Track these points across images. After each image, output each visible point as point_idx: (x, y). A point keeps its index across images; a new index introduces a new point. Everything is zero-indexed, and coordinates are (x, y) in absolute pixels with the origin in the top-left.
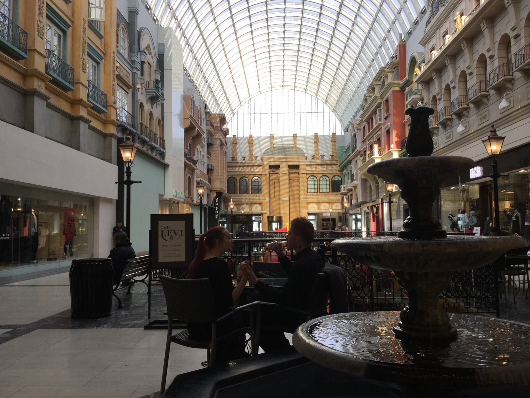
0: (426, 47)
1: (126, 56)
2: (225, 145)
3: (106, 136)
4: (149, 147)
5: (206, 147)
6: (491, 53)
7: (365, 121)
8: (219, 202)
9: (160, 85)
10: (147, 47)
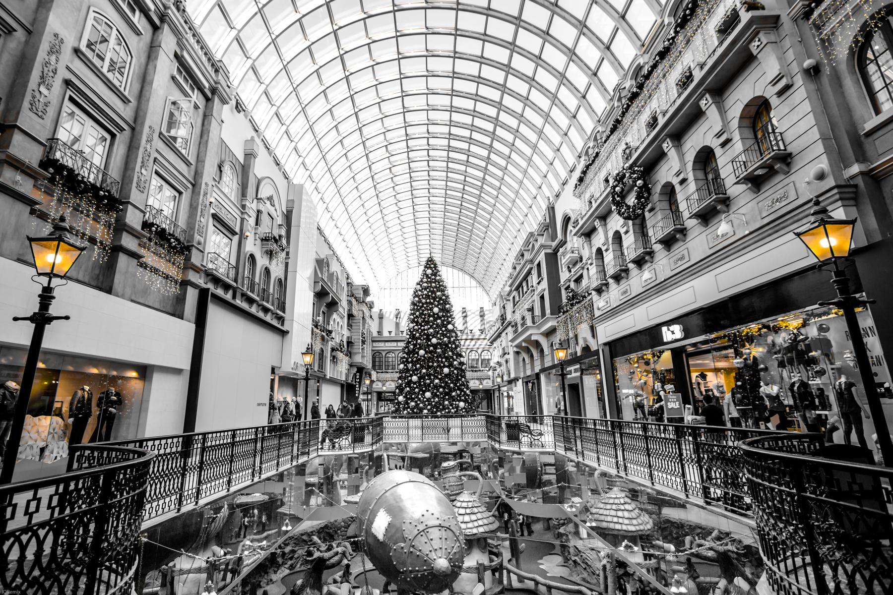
4: (261, 307)
5: (346, 319)
7: (514, 290)
8: (360, 378)
10: (268, 199)
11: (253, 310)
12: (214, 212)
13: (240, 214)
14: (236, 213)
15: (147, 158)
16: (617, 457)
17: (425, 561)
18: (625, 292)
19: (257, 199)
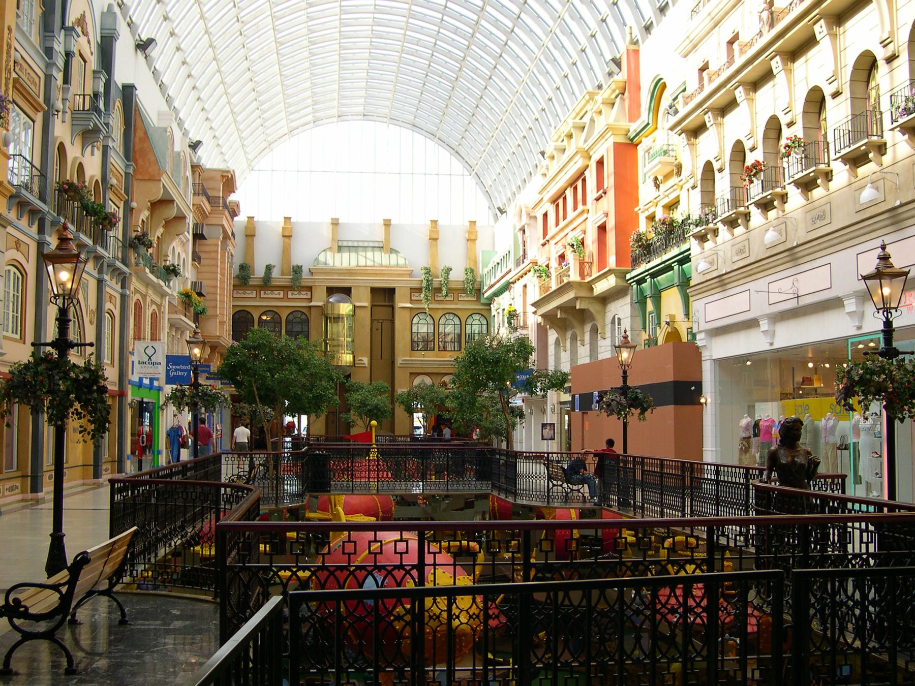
1: (35, 38)
2: (232, 238)
14: (37, 64)
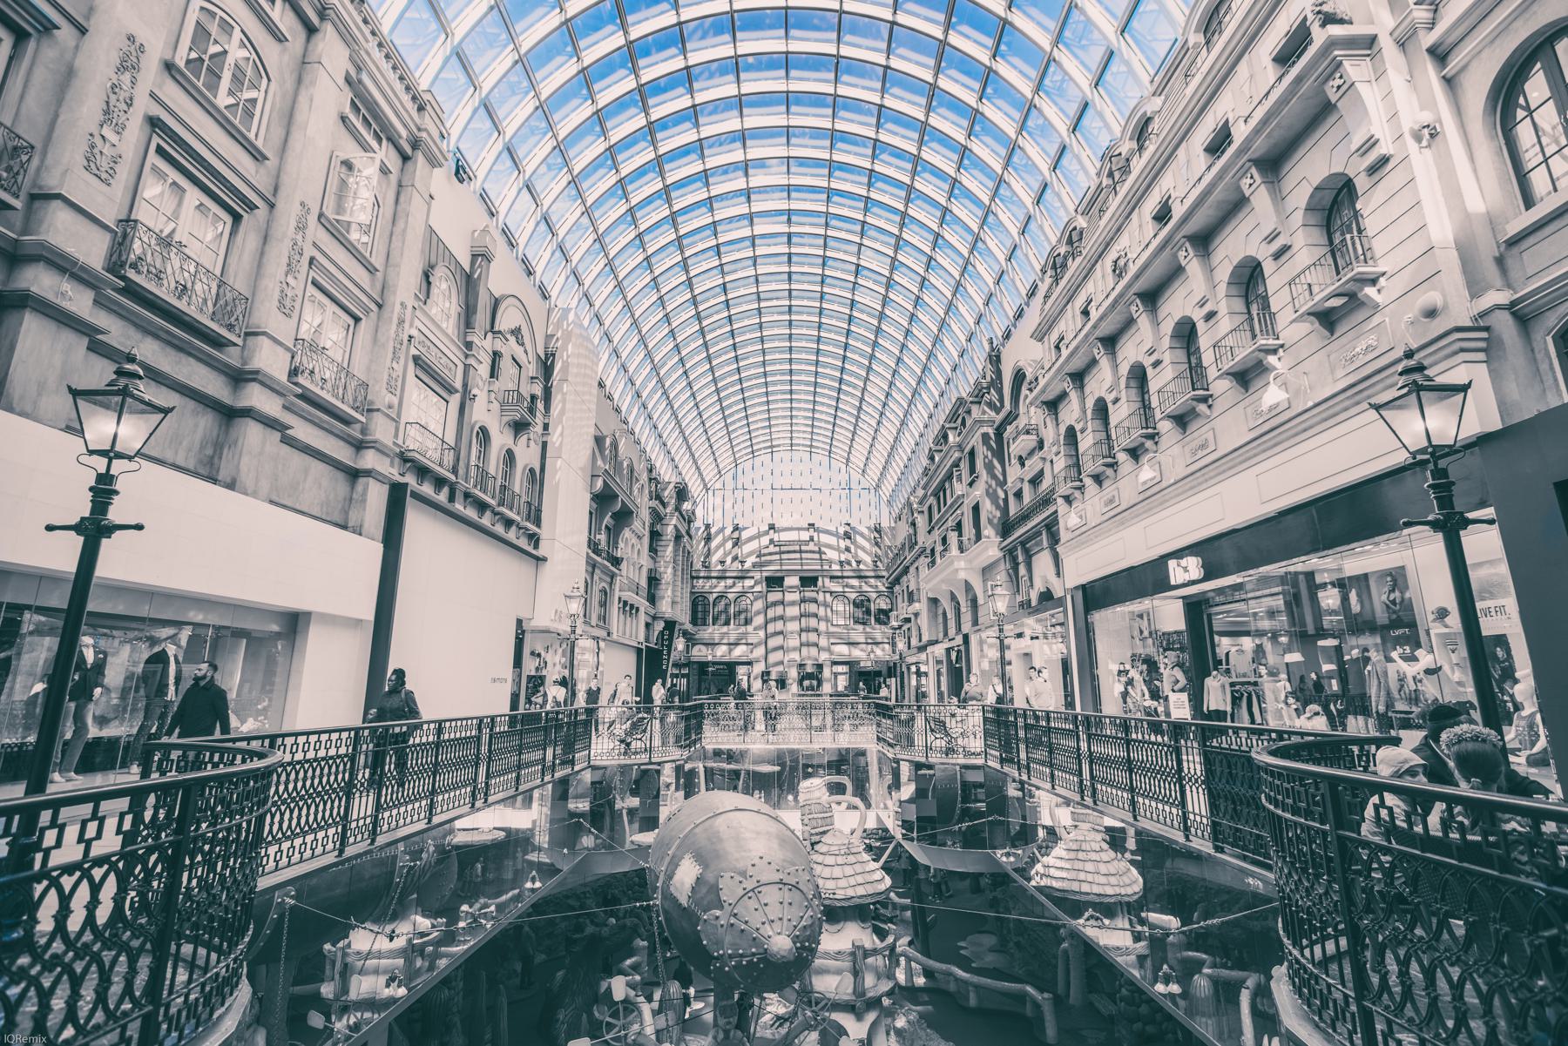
0: (1046, 343)
3: (354, 474)
5: (646, 540)
6: (1208, 308)
8: (671, 640)
9: (540, 405)
11: (486, 520)
12: (418, 353)
13: (463, 358)
14: (455, 353)
15: (297, 257)
16: (1080, 774)
17: (754, 939)
18: (1111, 501)
19: (494, 333)
